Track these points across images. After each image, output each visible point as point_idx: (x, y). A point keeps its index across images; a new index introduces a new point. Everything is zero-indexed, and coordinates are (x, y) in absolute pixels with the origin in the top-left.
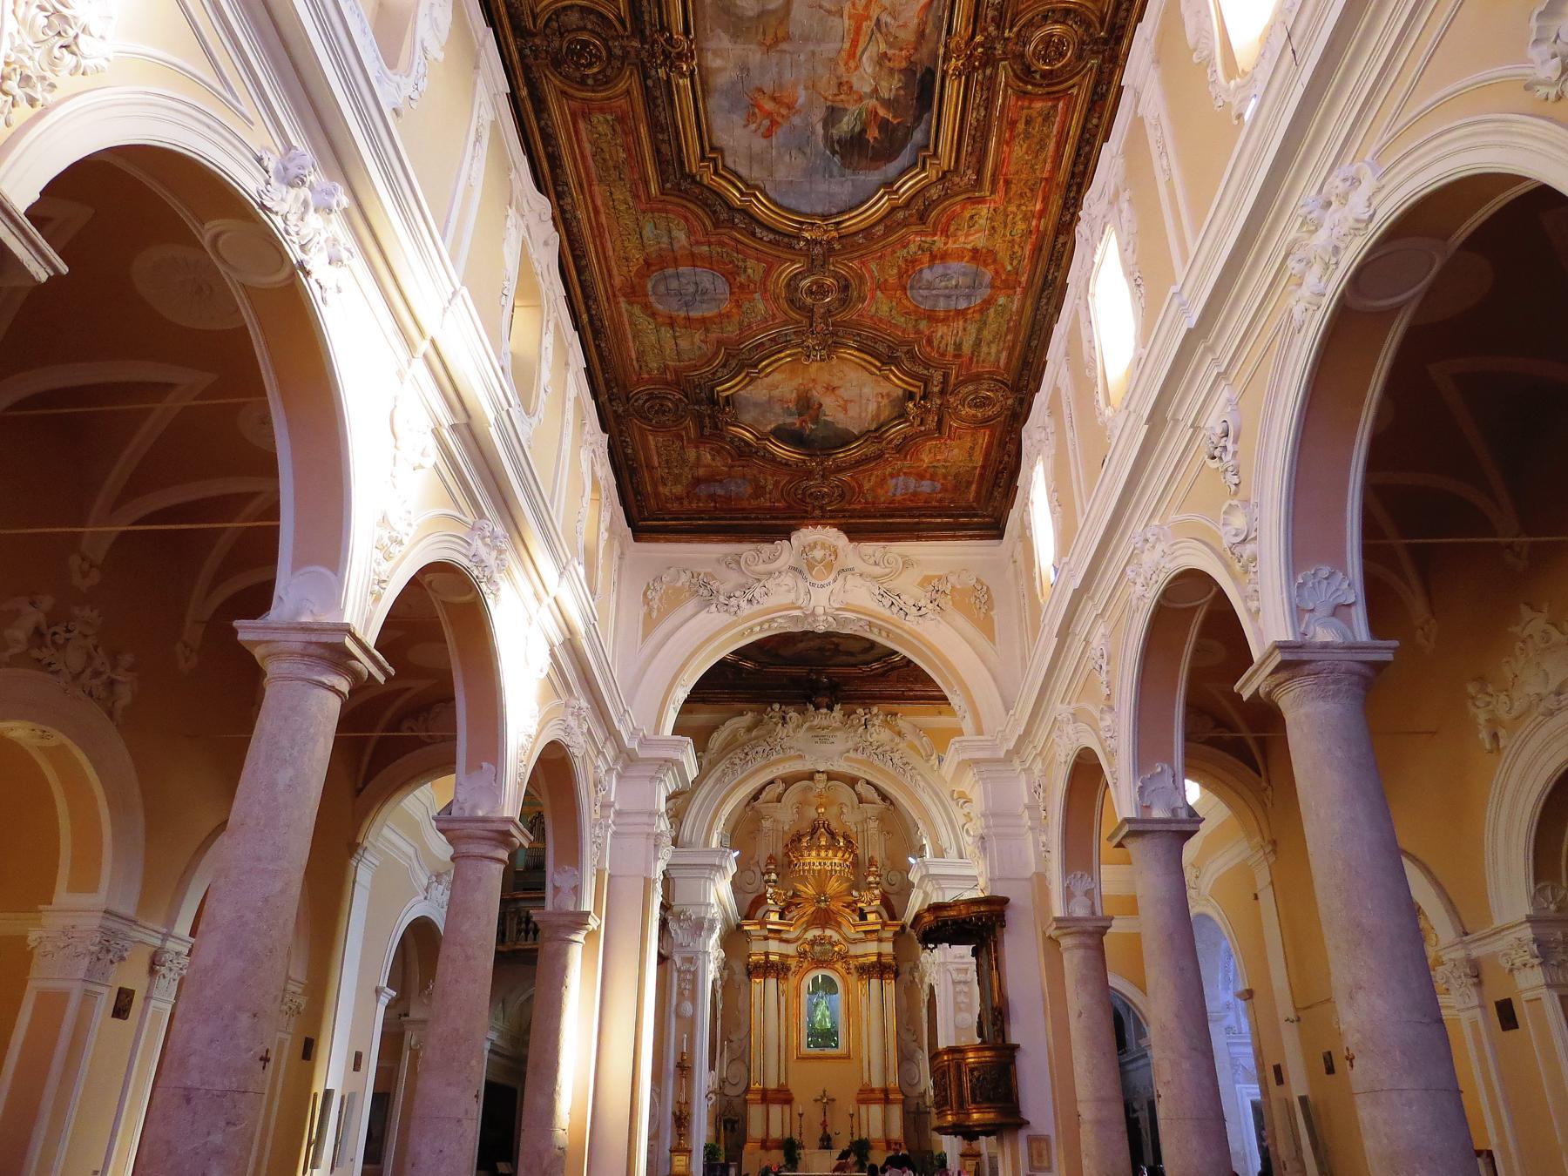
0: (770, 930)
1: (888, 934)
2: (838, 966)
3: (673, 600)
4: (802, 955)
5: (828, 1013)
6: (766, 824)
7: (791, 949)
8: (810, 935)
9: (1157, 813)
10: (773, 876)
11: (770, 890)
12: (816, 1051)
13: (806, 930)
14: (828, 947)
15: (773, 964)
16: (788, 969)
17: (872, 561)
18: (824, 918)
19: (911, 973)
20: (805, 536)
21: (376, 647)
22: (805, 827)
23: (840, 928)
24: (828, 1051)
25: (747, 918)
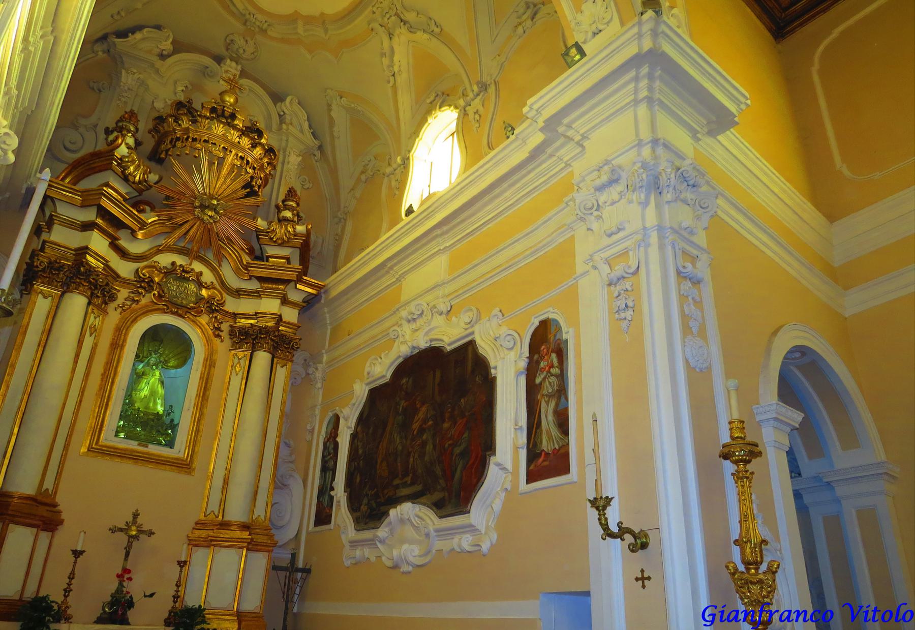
2: (204, 319)
4: (142, 283)
5: (161, 390)
6: (128, 79)
7: (125, 269)
8: (165, 260)
12: (133, 445)
13: (159, 251)
14: (192, 287)
15: (91, 270)
16: (113, 298)
19: (306, 364)
23: (220, 265)
24: (153, 449)
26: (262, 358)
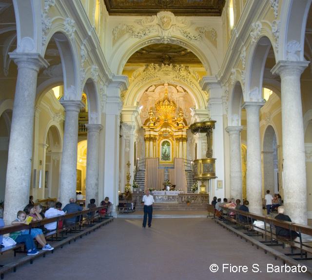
0: (151, 128)
1: (185, 129)
3: (122, 34)
4: (160, 135)
6: (150, 98)
8: (162, 130)
9: (254, 101)
10: (152, 113)
11: (151, 117)
13: (161, 128)
17: (181, 22)
18: (166, 125)
20: (161, 25)
21: (45, 58)
22: (162, 98)
25: (144, 125)
26: (181, 143)
